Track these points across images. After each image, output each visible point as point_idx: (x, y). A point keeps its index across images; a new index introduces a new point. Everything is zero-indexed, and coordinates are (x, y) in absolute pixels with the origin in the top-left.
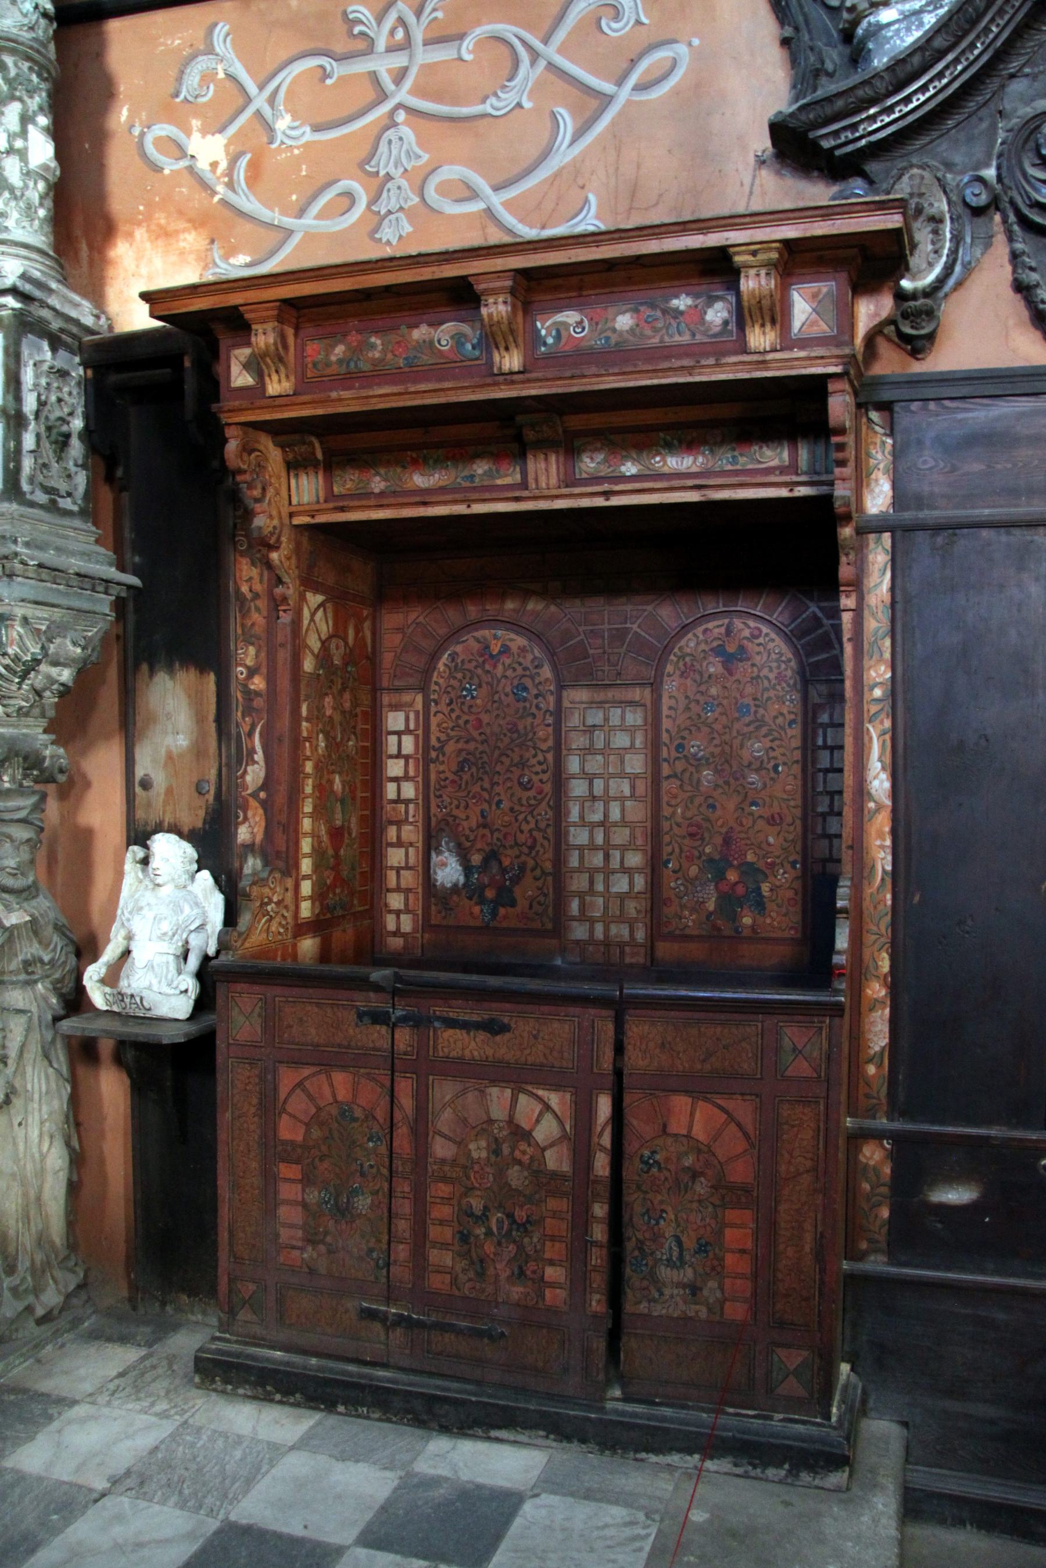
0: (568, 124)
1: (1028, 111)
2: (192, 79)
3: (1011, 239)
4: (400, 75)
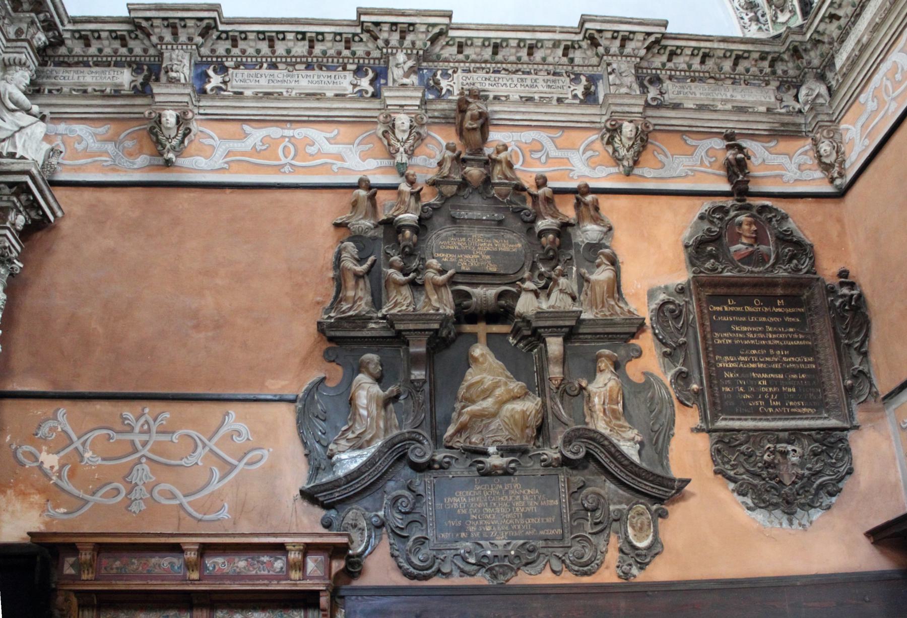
0: (217, 474)
1: (394, 494)
2: (45, 430)
3: (389, 537)
4: (145, 444)
